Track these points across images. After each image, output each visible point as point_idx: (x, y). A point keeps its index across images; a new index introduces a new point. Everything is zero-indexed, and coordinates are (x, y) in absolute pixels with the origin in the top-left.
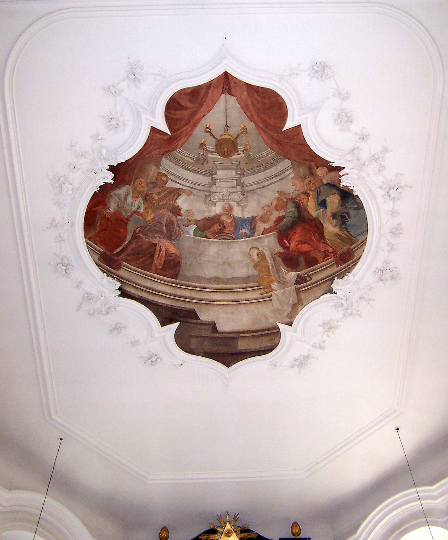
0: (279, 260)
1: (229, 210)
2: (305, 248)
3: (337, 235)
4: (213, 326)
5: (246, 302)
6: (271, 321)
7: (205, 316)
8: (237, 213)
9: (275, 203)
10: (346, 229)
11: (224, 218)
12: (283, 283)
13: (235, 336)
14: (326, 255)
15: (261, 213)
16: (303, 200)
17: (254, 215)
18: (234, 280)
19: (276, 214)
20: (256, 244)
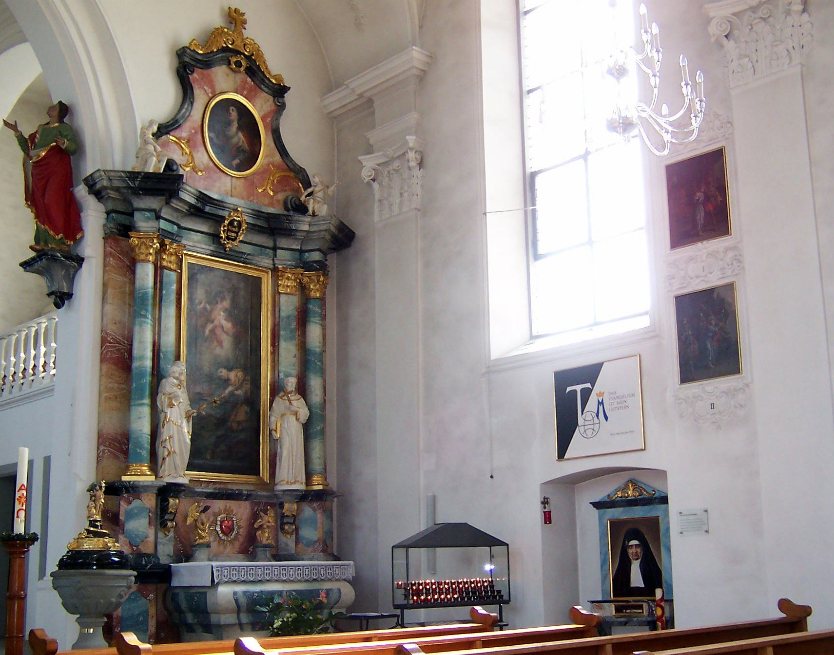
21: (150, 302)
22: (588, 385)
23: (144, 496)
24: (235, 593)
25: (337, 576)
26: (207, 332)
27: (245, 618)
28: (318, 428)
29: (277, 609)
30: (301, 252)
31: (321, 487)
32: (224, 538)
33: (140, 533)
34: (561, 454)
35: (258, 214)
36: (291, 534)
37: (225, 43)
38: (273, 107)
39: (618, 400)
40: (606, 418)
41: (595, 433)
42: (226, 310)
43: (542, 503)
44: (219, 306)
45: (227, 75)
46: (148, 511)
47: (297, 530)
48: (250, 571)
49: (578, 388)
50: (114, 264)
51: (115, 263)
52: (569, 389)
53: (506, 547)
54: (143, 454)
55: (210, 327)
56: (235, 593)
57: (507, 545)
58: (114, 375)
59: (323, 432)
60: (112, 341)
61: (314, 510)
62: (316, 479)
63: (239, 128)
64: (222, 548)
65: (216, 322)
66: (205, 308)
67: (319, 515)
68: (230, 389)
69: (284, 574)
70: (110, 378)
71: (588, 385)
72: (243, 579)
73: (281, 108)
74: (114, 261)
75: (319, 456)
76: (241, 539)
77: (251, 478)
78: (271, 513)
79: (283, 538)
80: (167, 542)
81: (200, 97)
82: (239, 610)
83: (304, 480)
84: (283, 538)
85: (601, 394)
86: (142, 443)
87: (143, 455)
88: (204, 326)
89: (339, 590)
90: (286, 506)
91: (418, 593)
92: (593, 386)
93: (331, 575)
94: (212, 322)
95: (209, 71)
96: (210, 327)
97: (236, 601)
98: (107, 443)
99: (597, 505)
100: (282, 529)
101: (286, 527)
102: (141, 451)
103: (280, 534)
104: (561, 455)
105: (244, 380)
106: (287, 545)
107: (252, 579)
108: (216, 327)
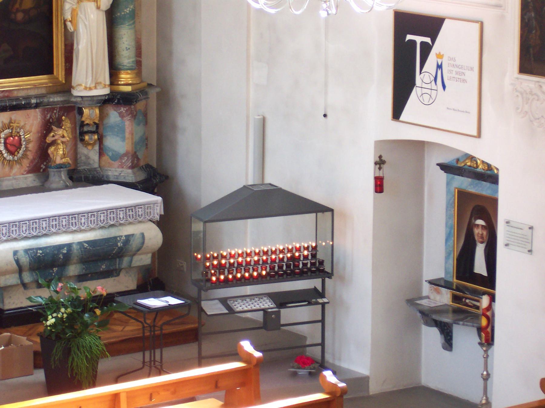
22: (428, 40)
24: (15, 253)
25: (140, 218)
27: (27, 277)
28: (127, 11)
29: (67, 260)
31: (129, 89)
32: (10, 157)
34: (397, 114)
36: (93, 145)
39: (458, 70)
40: (444, 87)
41: (431, 101)
43: (376, 163)
47: (100, 140)
48: (33, 225)
49: (419, 39)
52: (409, 37)
53: (329, 214)
56: (15, 253)
57: (332, 210)
59: (133, 15)
61: (121, 115)
62: (125, 77)
64: (7, 169)
67: (128, 123)
69: (74, 224)
71: (428, 40)
72: (25, 235)
75: (128, 47)
76: (30, 156)
77: (42, 79)
78: (67, 124)
79: (83, 150)
82: (20, 270)
83: (108, 82)
84: (83, 150)
85: (439, 56)
89: (143, 235)
90: (86, 111)
91: (220, 268)
92: (433, 41)
93: (133, 217)
97: (17, 261)
99: (444, 167)
100: (82, 140)
101: (87, 138)
103: (80, 145)
104: (397, 114)
106: (88, 158)
107: (35, 234)
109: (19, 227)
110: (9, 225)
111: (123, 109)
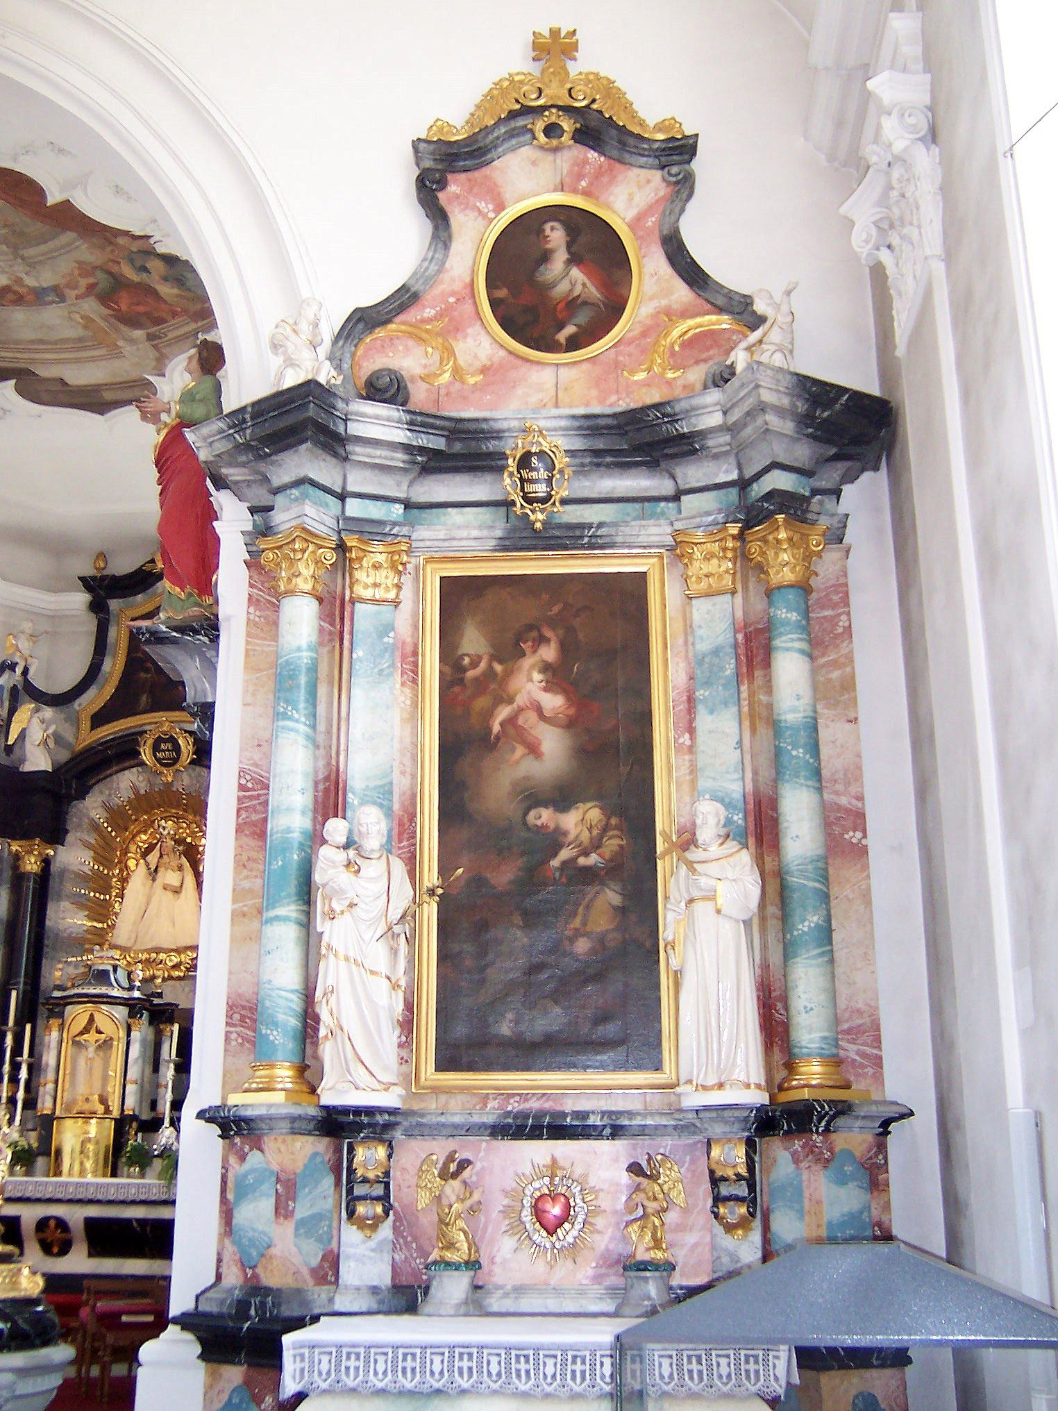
0: (113, 320)
1: (19, 281)
2: (141, 309)
3: (177, 296)
4: (63, 382)
5: (93, 359)
6: (134, 375)
7: (43, 372)
8: (30, 282)
9: (76, 272)
10: (189, 290)
11: (16, 288)
12: (132, 341)
13: (96, 389)
14: (175, 314)
15: (63, 281)
16: (115, 269)
17: (56, 283)
18: (66, 341)
19: (83, 282)
20: (73, 309)
21: (303, 680)
23: (269, 1143)
25: (726, 1384)
26: (496, 728)
30: (743, 484)
31: (806, 1094)
33: (256, 1235)
35: (590, 425)
37: (517, 101)
38: (663, 190)
42: (546, 668)
44: (527, 662)
45: (534, 163)
46: (274, 1179)
48: (404, 1359)
50: (257, 619)
51: (259, 617)
54: (272, 1038)
55: (504, 712)
58: (255, 861)
60: (250, 785)
62: (813, 1072)
63: (575, 259)
65: (520, 700)
66: (490, 673)
68: (565, 854)
69: (523, 1374)
70: (244, 866)
72: (380, 1385)
73: (683, 187)
74: (258, 613)
75: (809, 1006)
80: (372, 1254)
81: (460, 220)
86: (270, 1011)
87: (273, 1042)
88: (489, 714)
93: (701, 1379)
94: (511, 700)
95: (486, 171)
96: (504, 712)
98: (237, 1017)
102: (269, 1032)
105: (606, 829)
107: (409, 1385)
108: (521, 710)
109: (367, 1362)
110: (339, 1353)
111: (797, 1144)
